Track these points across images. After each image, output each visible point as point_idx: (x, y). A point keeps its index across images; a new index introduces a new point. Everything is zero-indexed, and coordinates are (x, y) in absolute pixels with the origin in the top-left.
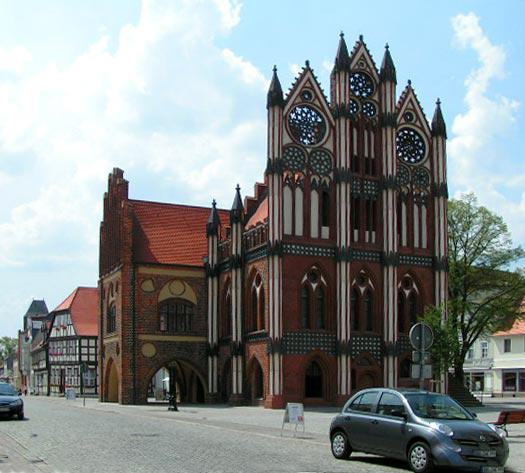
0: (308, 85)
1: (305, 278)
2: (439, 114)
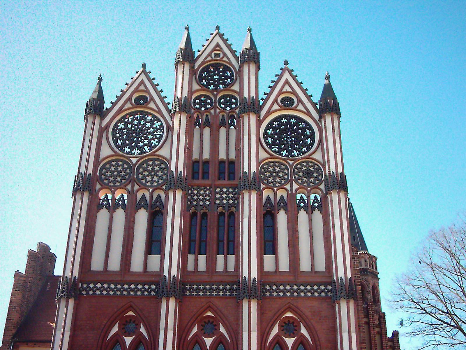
0: (142, 88)
1: (115, 329)
2: (328, 90)
